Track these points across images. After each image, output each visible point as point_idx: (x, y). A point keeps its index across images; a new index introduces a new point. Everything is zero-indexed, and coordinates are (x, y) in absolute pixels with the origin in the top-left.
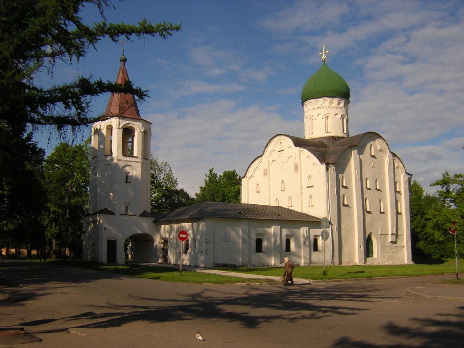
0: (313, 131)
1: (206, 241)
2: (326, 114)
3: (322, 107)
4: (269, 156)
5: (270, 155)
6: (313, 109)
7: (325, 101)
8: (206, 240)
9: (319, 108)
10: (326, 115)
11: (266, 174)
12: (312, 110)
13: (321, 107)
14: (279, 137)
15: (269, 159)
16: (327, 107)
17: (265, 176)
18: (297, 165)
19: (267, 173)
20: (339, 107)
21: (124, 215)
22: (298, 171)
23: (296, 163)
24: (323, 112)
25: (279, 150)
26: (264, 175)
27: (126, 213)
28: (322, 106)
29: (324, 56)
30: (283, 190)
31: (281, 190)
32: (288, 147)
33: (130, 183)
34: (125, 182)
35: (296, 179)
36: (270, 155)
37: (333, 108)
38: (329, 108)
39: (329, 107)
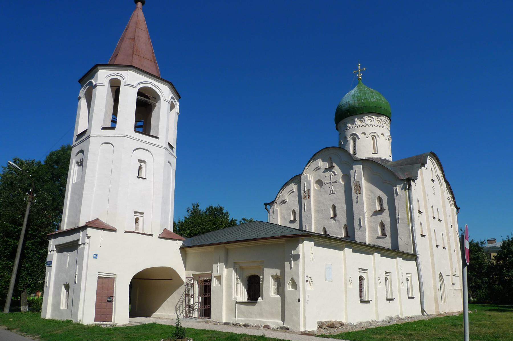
1: (306, 279)
2: (372, 133)
3: (367, 125)
6: (356, 126)
7: (371, 118)
8: (307, 277)
9: (363, 125)
10: (374, 134)
12: (354, 128)
13: (365, 124)
16: (373, 124)
20: (385, 127)
21: (133, 232)
24: (369, 130)
26: (304, 198)
27: (137, 228)
28: (366, 124)
29: (361, 75)
33: (146, 179)
34: (137, 177)
37: (379, 126)
38: (375, 126)
39: (374, 125)
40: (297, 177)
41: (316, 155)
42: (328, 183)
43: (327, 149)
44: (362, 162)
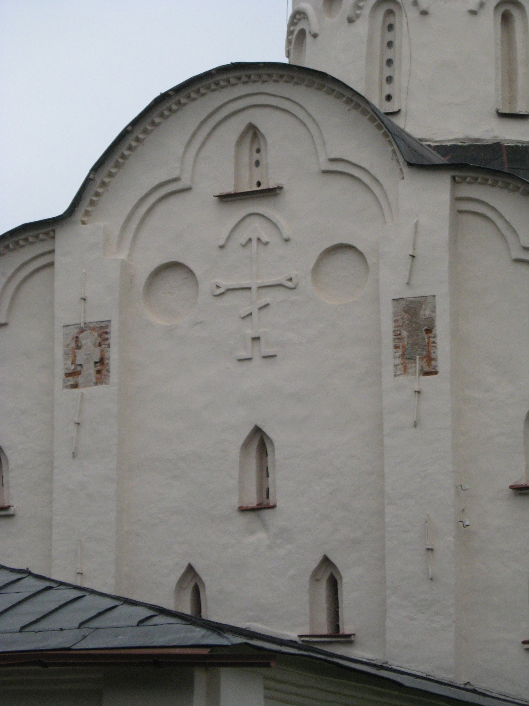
0: (389, 98)
4: (129, 235)
5: (134, 225)
11: (90, 370)
14: (241, 90)
15: (123, 256)
17: (75, 386)
18: (426, 312)
19: (102, 362)
22: (430, 359)
23: (409, 294)
25: (230, 189)
30: (252, 501)
31: (235, 502)
32: (325, 172)
35: (415, 425)
36: (134, 225)
40: (30, 235)
41: (163, 108)
42: (229, 290)
43: (238, 74)
44: (454, 178)
